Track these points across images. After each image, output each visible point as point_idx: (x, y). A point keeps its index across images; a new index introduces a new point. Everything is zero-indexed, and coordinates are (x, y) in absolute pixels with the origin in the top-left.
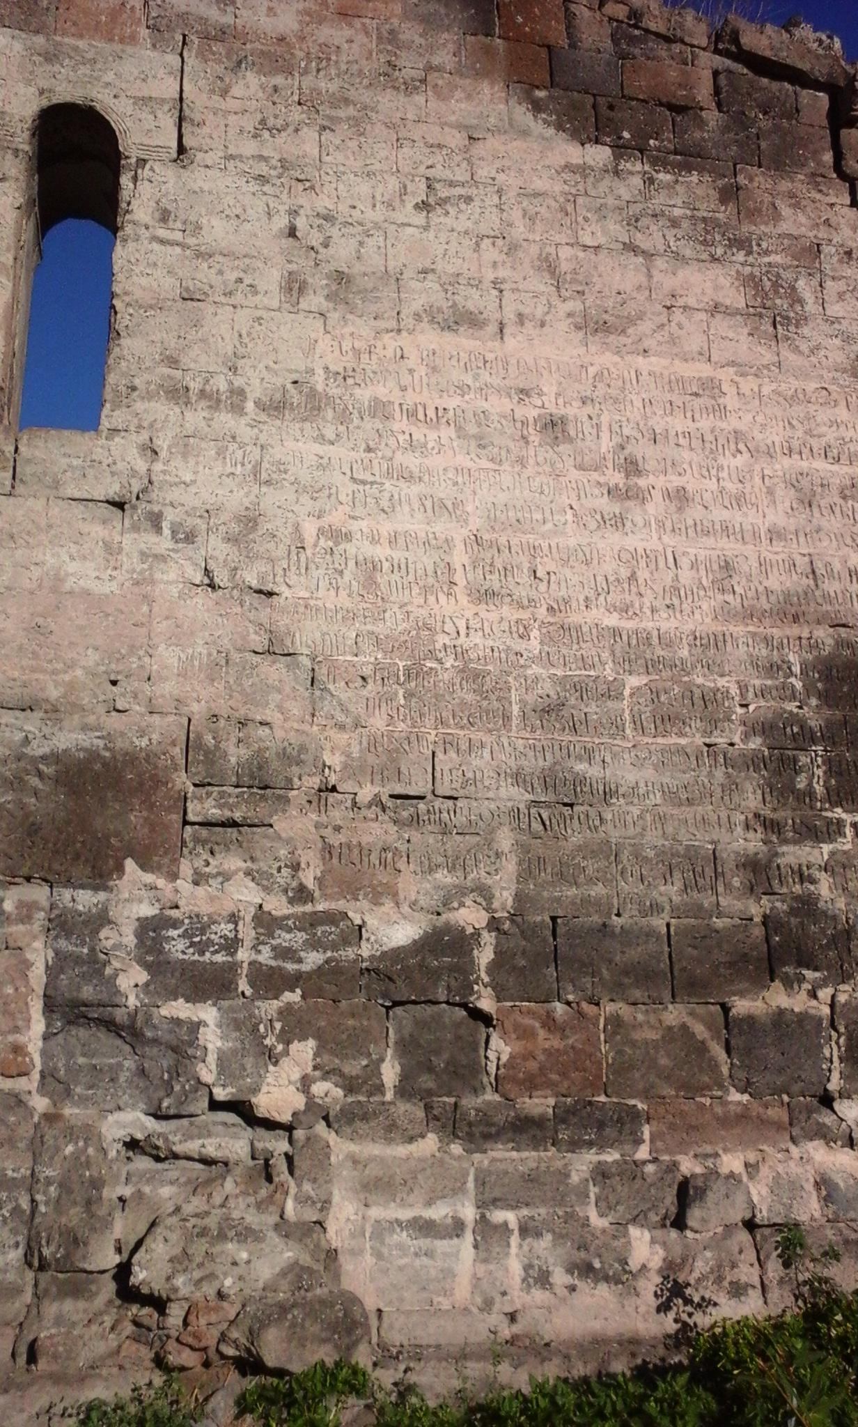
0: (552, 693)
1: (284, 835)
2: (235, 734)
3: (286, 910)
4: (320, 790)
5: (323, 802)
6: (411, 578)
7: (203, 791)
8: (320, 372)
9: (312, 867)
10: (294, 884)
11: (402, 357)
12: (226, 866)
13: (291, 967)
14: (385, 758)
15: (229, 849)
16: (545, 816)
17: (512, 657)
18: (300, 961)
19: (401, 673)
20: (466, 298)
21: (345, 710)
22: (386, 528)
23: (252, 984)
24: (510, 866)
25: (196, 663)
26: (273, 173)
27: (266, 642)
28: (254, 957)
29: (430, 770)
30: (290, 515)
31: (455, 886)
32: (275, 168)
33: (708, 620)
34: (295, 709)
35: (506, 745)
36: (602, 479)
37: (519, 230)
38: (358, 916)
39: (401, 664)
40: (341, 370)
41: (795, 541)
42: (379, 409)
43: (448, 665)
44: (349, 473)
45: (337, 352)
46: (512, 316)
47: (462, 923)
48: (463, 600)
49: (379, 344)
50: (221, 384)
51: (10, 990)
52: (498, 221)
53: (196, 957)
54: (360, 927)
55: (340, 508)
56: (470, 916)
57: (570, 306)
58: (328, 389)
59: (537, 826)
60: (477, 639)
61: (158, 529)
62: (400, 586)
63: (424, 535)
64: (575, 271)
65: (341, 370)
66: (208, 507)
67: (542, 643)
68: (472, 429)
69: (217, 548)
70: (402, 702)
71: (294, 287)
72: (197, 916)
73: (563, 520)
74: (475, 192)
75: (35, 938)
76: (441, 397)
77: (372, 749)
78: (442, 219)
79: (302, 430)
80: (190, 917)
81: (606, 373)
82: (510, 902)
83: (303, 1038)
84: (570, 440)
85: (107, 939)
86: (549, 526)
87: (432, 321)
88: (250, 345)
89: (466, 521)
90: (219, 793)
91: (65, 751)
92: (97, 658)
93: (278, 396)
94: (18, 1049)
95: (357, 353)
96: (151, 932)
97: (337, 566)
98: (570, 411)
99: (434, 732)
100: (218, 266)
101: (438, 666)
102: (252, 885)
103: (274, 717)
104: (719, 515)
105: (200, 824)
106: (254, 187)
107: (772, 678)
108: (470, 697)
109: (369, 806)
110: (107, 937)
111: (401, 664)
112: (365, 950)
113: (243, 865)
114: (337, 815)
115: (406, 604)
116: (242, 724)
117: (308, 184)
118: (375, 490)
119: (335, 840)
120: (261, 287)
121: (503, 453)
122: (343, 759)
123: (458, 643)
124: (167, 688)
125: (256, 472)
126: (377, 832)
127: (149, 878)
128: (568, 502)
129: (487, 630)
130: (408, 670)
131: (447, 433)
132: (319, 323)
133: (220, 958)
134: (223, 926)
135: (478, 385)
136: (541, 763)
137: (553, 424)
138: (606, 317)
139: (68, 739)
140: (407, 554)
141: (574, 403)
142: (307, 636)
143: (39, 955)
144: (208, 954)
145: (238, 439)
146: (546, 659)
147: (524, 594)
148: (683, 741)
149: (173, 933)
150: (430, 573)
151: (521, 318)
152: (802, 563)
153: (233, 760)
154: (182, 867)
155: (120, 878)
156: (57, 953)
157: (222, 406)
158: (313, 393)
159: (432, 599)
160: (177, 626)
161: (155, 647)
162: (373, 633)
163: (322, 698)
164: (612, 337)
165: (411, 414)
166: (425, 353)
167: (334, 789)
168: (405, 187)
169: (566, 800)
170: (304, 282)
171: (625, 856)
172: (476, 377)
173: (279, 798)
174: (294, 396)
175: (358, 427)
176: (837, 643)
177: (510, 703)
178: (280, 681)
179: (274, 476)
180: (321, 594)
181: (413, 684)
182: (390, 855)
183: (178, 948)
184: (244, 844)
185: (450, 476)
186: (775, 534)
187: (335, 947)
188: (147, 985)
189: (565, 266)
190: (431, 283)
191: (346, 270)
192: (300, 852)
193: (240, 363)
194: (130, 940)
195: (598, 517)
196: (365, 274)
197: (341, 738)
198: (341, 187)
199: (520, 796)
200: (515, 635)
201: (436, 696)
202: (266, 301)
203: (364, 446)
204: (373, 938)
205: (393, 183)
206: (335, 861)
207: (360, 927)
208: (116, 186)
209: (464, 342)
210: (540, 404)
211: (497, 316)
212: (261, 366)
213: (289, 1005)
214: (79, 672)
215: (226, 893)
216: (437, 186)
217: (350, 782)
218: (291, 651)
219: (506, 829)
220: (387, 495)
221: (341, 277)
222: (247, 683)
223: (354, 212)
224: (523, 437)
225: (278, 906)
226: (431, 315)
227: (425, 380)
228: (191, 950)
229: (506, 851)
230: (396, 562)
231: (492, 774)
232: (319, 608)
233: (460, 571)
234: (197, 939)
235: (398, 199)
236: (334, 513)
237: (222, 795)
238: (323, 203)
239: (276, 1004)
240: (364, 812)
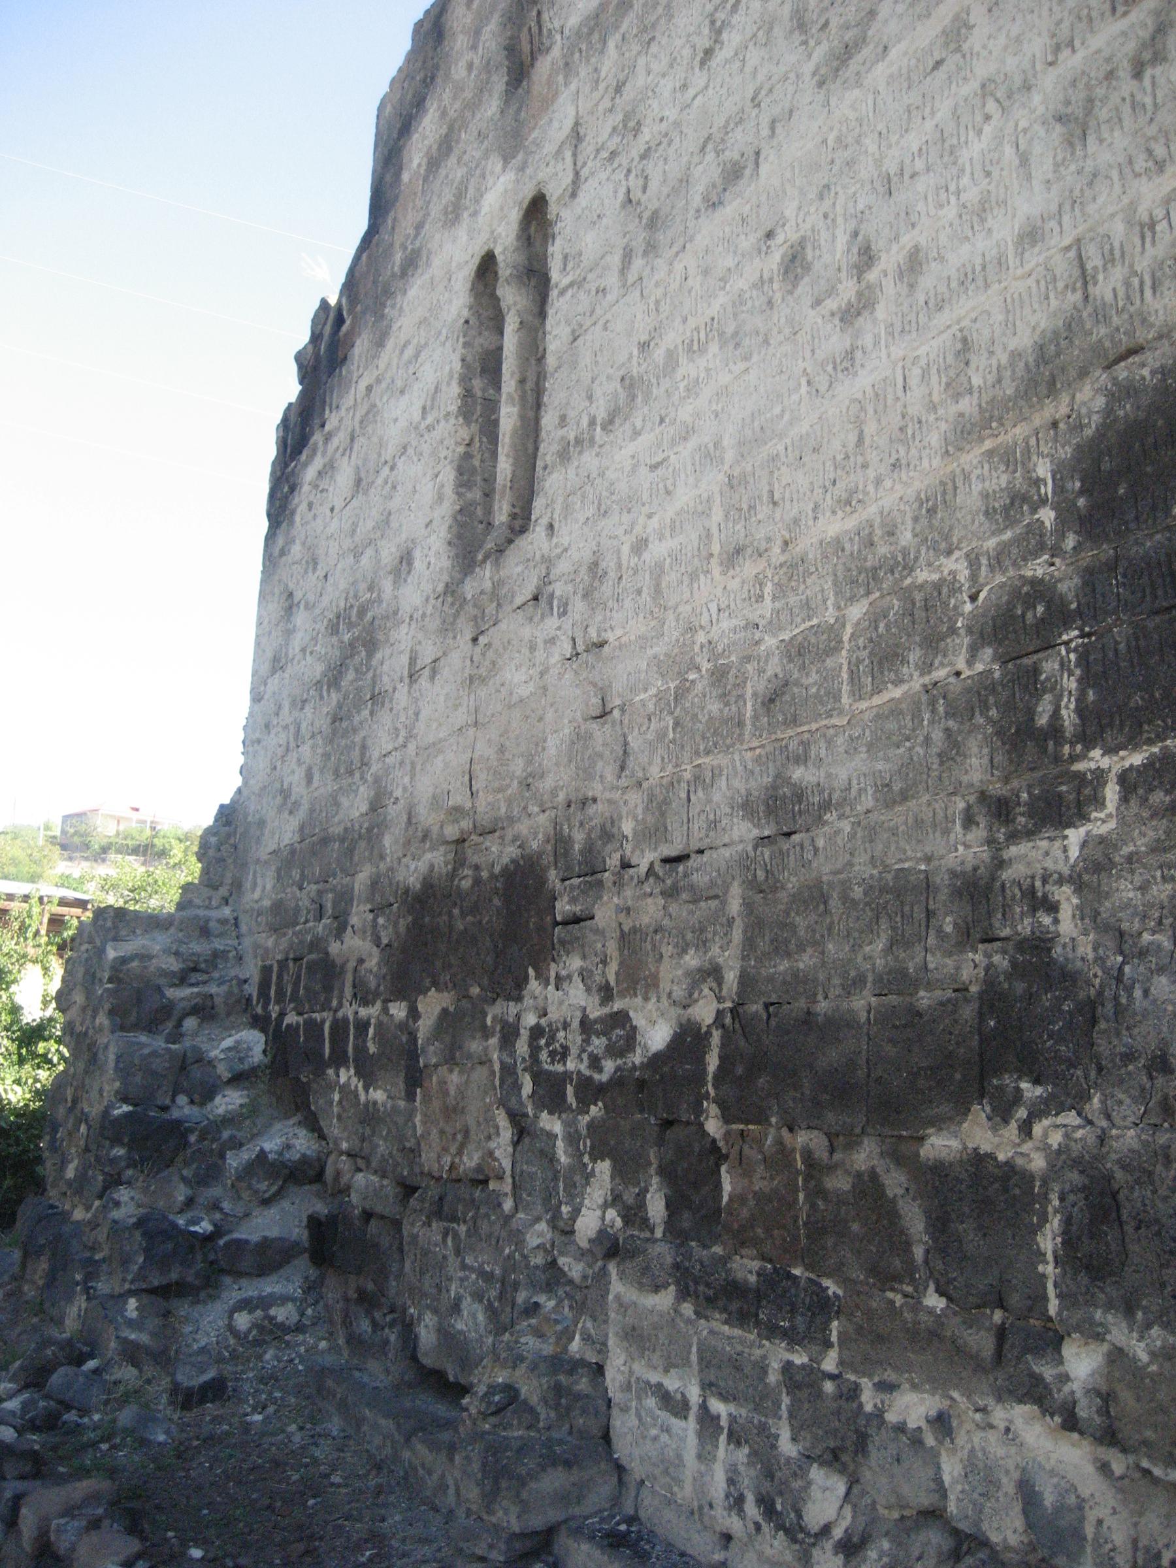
13: (596, 1076)
18: (600, 1070)
24: (737, 935)
33: (936, 462)
41: (1057, 229)
59: (761, 875)
60: (726, 624)
68: (730, 329)
83: (603, 1160)
94: (491, 1154)
103: (595, 789)
104: (960, 256)
107: (1010, 522)
108: (714, 707)
112: (637, 1058)
116: (583, 803)
124: (548, 783)
126: (651, 911)
133: (559, 1068)
146: (774, 626)
148: (897, 693)
152: (1063, 267)
164: (854, 65)
171: (834, 903)
176: (1111, 397)
186: (1031, 236)
187: (621, 1053)
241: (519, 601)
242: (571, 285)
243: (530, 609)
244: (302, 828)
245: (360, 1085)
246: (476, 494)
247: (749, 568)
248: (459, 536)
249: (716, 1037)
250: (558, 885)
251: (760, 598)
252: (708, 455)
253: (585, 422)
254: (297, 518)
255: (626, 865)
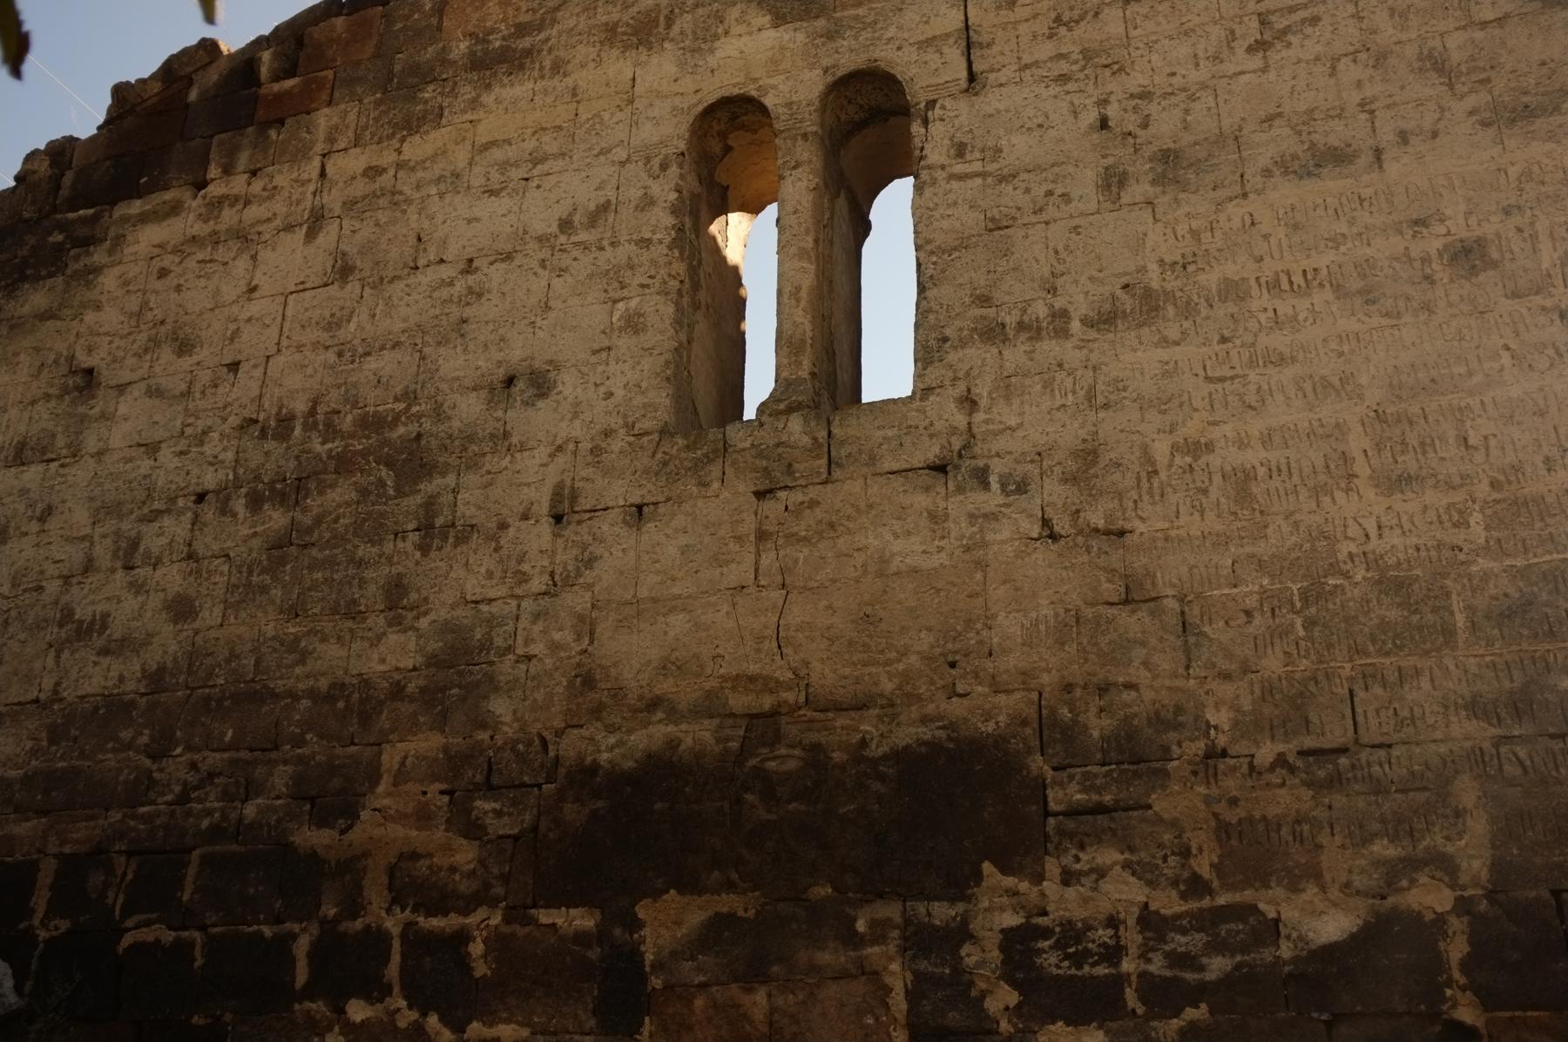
0: (1512, 591)
1: (1166, 816)
2: (1095, 703)
3: (1179, 907)
4: (1207, 756)
5: (1211, 771)
6: (1296, 479)
7: (1065, 774)
8: (1153, 267)
9: (1205, 854)
10: (1186, 874)
11: (1253, 224)
12: (1099, 860)
13: (1190, 976)
14: (1288, 707)
15: (1100, 841)
16: (1522, 754)
17: (1446, 553)
18: (1202, 969)
19: (1296, 598)
20: (1326, 134)
21: (1229, 655)
22: (1256, 426)
23: (1143, 999)
24: (1479, 826)
25: (1042, 628)
26: (1074, 68)
27: (1123, 589)
28: (1143, 966)
29: (1348, 712)
30: (1135, 437)
31: (1402, 860)
32: (1076, 62)
34: (1165, 663)
35: (1452, 667)
36: (1549, 303)
37: (1388, 32)
38: (1273, 908)
39: (1295, 588)
40: (1179, 258)
42: (1233, 290)
43: (1358, 578)
44: (1202, 373)
45: (1172, 241)
46: (1391, 137)
47: (1415, 906)
48: (1370, 493)
49: (1222, 217)
50: (1041, 310)
51: (870, 1021)
52: (1357, 33)
53: (1073, 971)
54: (1277, 921)
55: (1196, 415)
56: (1429, 897)
57: (1471, 101)
58: (1165, 284)
59: (1511, 770)
60: (1395, 539)
61: (986, 486)
62: (1282, 493)
63: (1306, 424)
64: (1472, 58)
65: (1179, 258)
66: (1039, 449)
67: (1487, 528)
68: (1356, 284)
69: (1054, 492)
70: (1302, 633)
71: (1113, 182)
72: (1070, 922)
73: (1497, 366)
74: (1323, 9)
75: (891, 959)
76: (1308, 257)
77: (1269, 698)
78: (1284, 53)
79: (1139, 337)
80: (1061, 924)
81: (1536, 168)
82: (1484, 875)
84: (1494, 265)
85: (968, 955)
86: (1478, 378)
87: (1286, 173)
88: (1069, 260)
89: (1361, 397)
90: (1084, 774)
91: (907, 747)
92: (932, 639)
93: (1107, 307)
95: (1195, 234)
96: (1018, 944)
97: (1199, 484)
98: (1489, 229)
99: (1348, 666)
100: (1023, 185)
101: (1346, 583)
102: (1132, 879)
103: (1143, 676)
105: (1065, 814)
106: (1055, 89)
109: (1272, 768)
110: (970, 955)
111: (1295, 588)
112: (1286, 951)
113: (1121, 857)
114: (1231, 784)
115: (1292, 513)
116: (1103, 689)
117: (1116, 67)
118: (1237, 384)
119: (1232, 816)
120: (1075, 193)
121: (1401, 304)
122: (1232, 715)
123: (1370, 547)
124: (1012, 661)
125: (1091, 395)
126: (1285, 800)
127: (1010, 881)
128: (1502, 342)
129: (1407, 526)
130: (1305, 597)
131: (1322, 297)
132: (1147, 215)
133: (1102, 970)
134: (1101, 932)
135: (1355, 230)
136: (1507, 685)
137: (1467, 251)
138: (1525, 99)
139: (907, 734)
140: (1287, 452)
141: (1493, 219)
142: (1170, 573)
143: (897, 977)
144: (1087, 968)
145: (1066, 366)
147: (1453, 470)
149: (1046, 944)
150: (1320, 464)
151: (1404, 137)
153: (1096, 734)
154: (1048, 866)
155: (978, 884)
156: (917, 975)
157: (1044, 333)
158: (1148, 293)
159: (1326, 500)
160: (1017, 590)
161: (994, 616)
162: (1254, 556)
163: (1197, 645)
165: (1274, 286)
166: (1281, 212)
167: (1224, 754)
168: (1233, 32)
169: (1552, 730)
170: (1125, 173)
172: (1352, 222)
173: (1156, 772)
174: (1127, 302)
175: (1208, 318)
177: (1452, 613)
178: (1143, 632)
179: (1112, 397)
180: (1182, 522)
181: (1313, 610)
182: (1306, 828)
183: (1051, 961)
184: (1120, 832)
185: (1334, 346)
187: (1244, 949)
188: (1019, 1006)
189: (1456, 57)
190: (1280, 130)
191: (1172, 146)
192: (1185, 836)
193: (1059, 282)
194: (995, 955)
195: (1550, 352)
196: (1196, 144)
197: (1228, 690)
198: (1154, 57)
199: (1481, 732)
200: (1447, 524)
201: (1346, 619)
202: (1081, 206)
203: (1217, 338)
204: (1295, 935)
205: (1217, 33)
206: (1234, 842)
207: (1277, 921)
208: (908, 136)
209: (1333, 184)
210: (1443, 231)
211: (1371, 142)
212: (1083, 279)
213: (1191, 1022)
214: (913, 659)
215: (1103, 890)
216: (1273, 18)
217: (1244, 742)
218: (1154, 595)
219: (1466, 777)
220: (1253, 388)
221: (1168, 157)
222: (1104, 642)
223: (1175, 81)
224: (1427, 278)
225: (1169, 903)
226: (1286, 167)
227: (1285, 242)
228: (1066, 963)
229: (1470, 806)
230: (1274, 463)
231: (1436, 708)
232: (1181, 537)
233: (1360, 459)
234: (1071, 950)
235: (1225, 49)
236: (1189, 424)
237: (1086, 776)
238: (1136, 80)
239: (1175, 1023)
240: (1268, 777)
241: (889, 464)
242: (983, 175)
243: (926, 477)
244: (156, 679)
245: (433, 1021)
246: (683, 337)
247: (1435, 499)
248: (675, 375)
249: (1457, 924)
250: (1049, 774)
251: (1462, 524)
252: (1326, 384)
253: (1041, 310)
254: (109, 281)
255: (1215, 754)
